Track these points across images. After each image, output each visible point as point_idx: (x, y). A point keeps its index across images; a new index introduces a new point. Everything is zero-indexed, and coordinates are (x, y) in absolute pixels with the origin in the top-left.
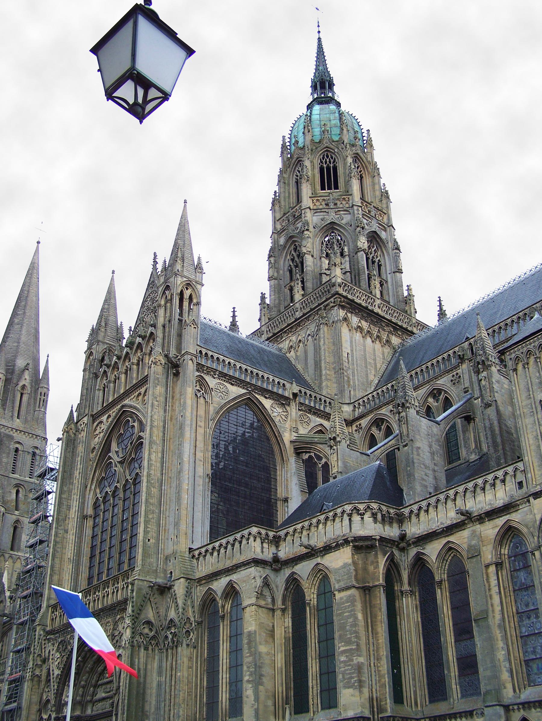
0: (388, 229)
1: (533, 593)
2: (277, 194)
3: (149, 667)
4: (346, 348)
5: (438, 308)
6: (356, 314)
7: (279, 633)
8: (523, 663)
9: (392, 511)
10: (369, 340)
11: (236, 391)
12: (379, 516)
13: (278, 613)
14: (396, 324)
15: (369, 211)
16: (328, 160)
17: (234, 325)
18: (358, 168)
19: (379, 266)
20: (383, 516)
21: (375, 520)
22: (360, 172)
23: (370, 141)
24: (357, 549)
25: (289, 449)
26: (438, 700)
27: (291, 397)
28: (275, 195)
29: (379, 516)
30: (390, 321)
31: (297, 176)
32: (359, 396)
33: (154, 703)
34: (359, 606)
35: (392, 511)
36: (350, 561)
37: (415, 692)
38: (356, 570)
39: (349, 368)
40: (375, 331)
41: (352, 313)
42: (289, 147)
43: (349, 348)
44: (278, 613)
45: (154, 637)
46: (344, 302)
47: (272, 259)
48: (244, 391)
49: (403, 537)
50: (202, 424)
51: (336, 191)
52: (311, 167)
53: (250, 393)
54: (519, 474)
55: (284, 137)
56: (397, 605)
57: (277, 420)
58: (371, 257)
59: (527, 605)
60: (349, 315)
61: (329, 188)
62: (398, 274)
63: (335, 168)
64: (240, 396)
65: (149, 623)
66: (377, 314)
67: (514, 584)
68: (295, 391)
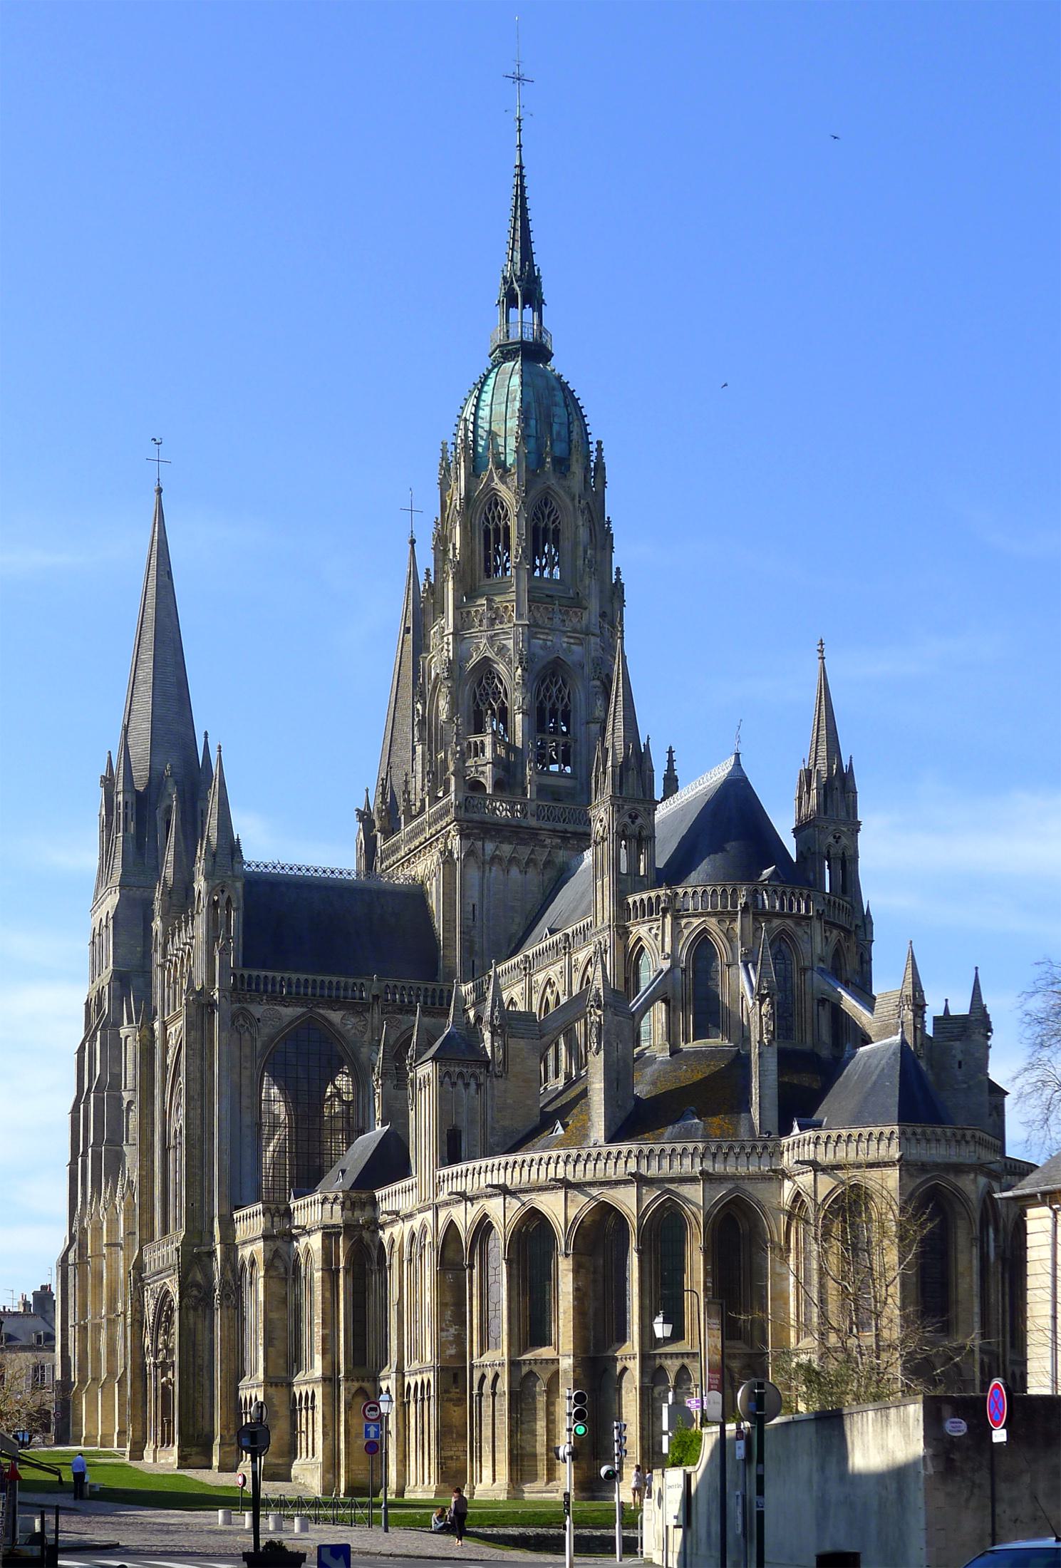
3: (200, 1326)
6: (492, 839)
7: (291, 1299)
9: (363, 1196)
10: (515, 871)
11: (289, 1012)
13: (290, 1282)
14: (566, 832)
24: (326, 1236)
29: (348, 1203)
33: (206, 1357)
35: (363, 1196)
39: (474, 926)
40: (524, 852)
41: (483, 839)
43: (476, 894)
44: (290, 1282)
45: (201, 1300)
46: (468, 828)
48: (300, 1010)
50: (248, 1065)
58: (548, 706)
64: (298, 1018)
65: (198, 1286)
68: (375, 992)
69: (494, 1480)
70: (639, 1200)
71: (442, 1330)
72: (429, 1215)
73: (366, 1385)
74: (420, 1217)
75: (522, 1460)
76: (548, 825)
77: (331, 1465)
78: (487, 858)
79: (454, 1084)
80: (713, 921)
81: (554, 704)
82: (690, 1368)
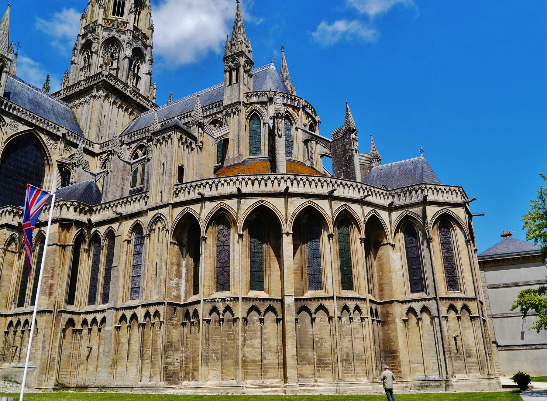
1: (141, 256)
4: (105, 112)
6: (115, 95)
8: (130, 289)
10: (120, 109)
11: (23, 128)
12: (78, 210)
15: (139, 35)
19: (138, 68)
20: (81, 209)
21: (75, 211)
25: (55, 164)
26: (91, 304)
27: (61, 135)
29: (78, 210)
30: (136, 101)
32: (107, 140)
34: (58, 254)
36: (57, 231)
37: (81, 299)
38: (60, 236)
41: (112, 93)
49: (90, 221)
53: (33, 130)
54: (146, 199)
56: (80, 255)
57: (49, 148)
59: (137, 262)
60: (110, 94)
61: (118, 15)
63: (124, 3)
66: (128, 96)
67: (135, 251)
68: (64, 132)
69: (222, 379)
70: (331, 208)
71: (171, 279)
72: (165, 211)
73: (75, 317)
74: (151, 214)
75: (247, 366)
76: (135, 99)
77: (46, 368)
78: (112, 100)
79: (183, 144)
80: (291, 109)
81: (135, 63)
82: (361, 307)
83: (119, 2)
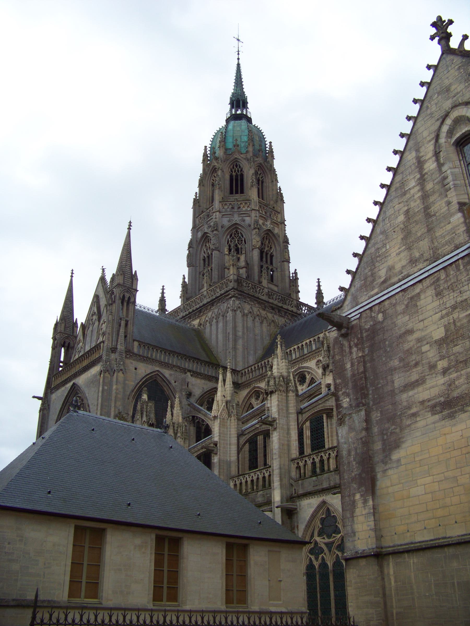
0: (280, 226)
2: (198, 195)
5: (317, 288)
16: (237, 169)
17: (162, 301)
18: (260, 174)
22: (262, 177)
23: (271, 151)
28: (196, 197)
31: (213, 180)
42: (209, 155)
47: (191, 249)
51: (242, 195)
52: (224, 176)
55: (206, 147)
61: (237, 193)
62: (285, 263)
63: (242, 175)
83: (237, 176)
